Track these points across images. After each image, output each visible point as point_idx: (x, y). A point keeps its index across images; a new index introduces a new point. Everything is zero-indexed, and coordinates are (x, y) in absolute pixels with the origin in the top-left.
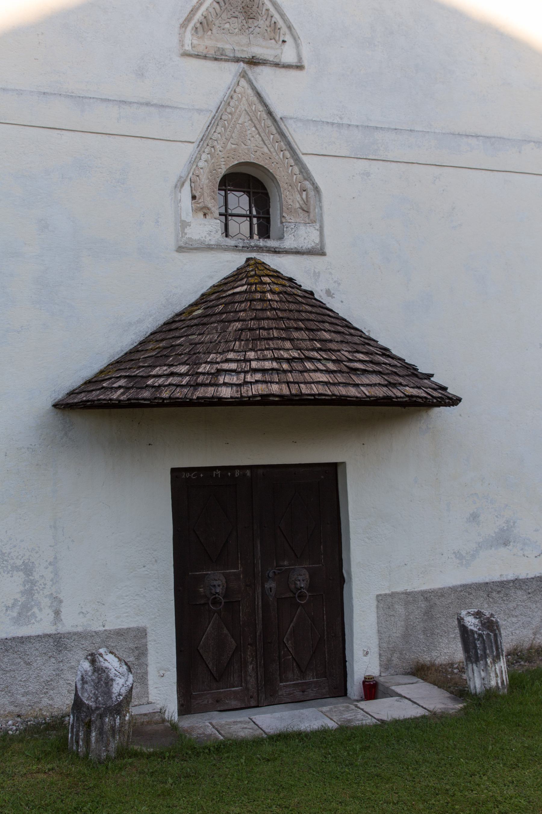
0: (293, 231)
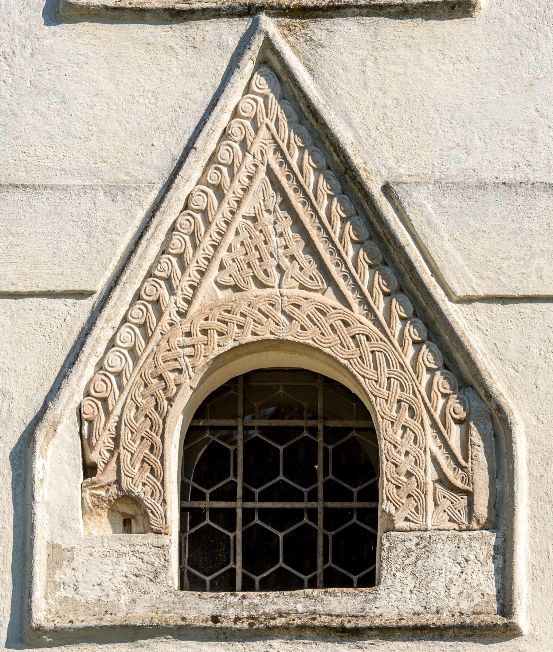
0: (413, 558)
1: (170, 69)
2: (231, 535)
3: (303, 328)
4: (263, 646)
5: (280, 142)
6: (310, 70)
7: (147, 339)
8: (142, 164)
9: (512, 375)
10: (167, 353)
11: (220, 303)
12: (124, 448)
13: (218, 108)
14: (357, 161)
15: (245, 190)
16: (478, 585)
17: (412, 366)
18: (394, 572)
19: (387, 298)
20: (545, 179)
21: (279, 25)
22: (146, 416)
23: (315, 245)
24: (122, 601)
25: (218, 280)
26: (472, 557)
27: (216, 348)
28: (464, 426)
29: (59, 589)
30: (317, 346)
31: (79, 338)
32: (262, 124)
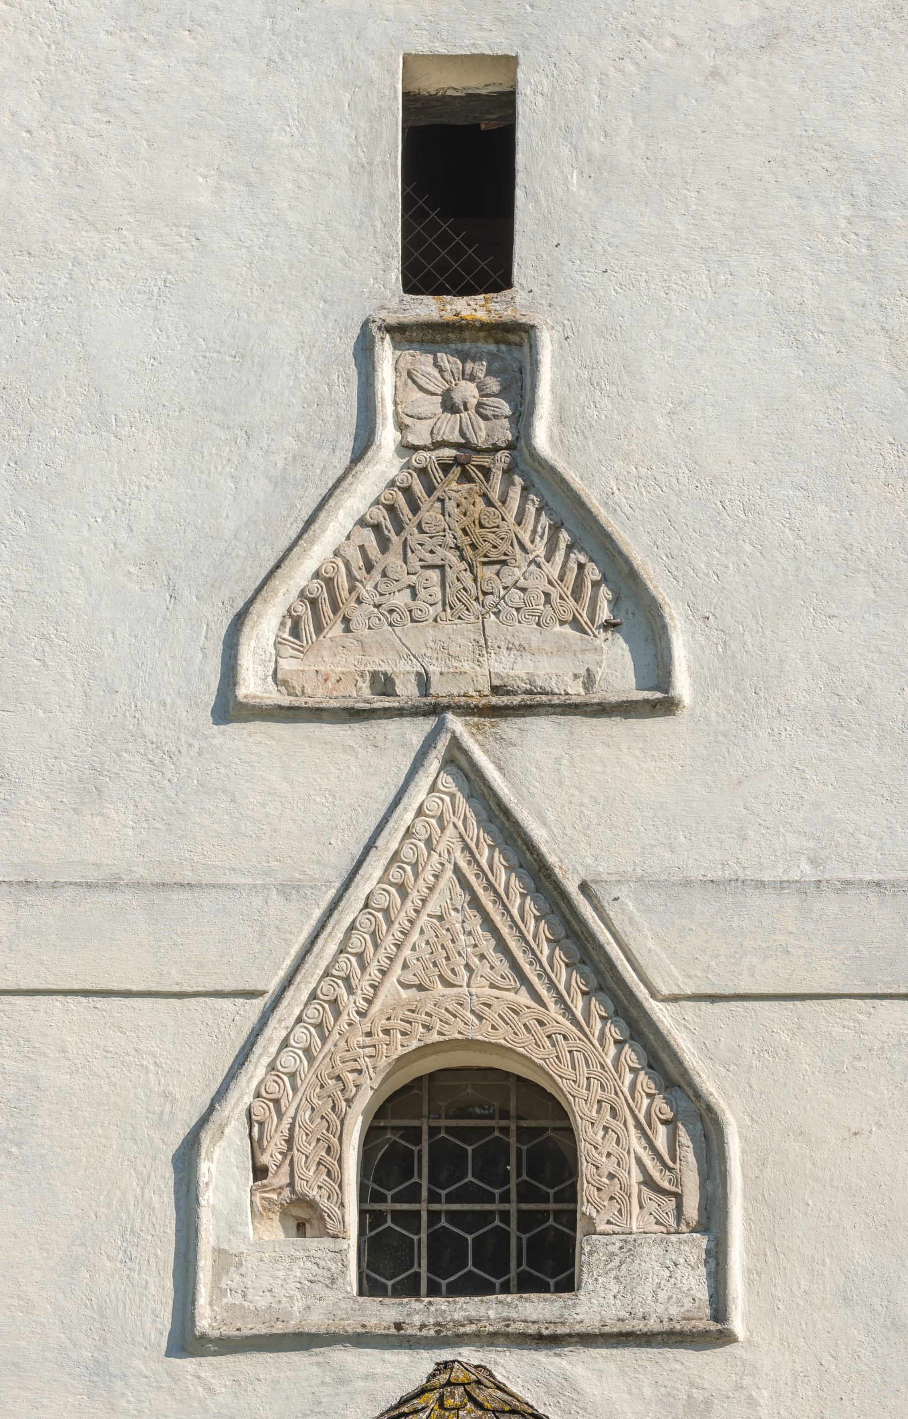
0: (616, 1262)
1: (349, 768)
2: (415, 1238)
3: (493, 1027)
4: (451, 1354)
5: (468, 841)
6: (500, 769)
7: (324, 1039)
8: (318, 863)
9: (723, 1074)
10: (346, 1053)
11: (403, 1003)
12: (298, 1150)
13: (401, 807)
14: (552, 859)
15: (431, 889)
16: (689, 1290)
17: (614, 1066)
18: (595, 1276)
19: (586, 997)
20: (756, 877)
21: (467, 724)
22: (323, 1117)
23: (507, 944)
24: (295, 1308)
25: (401, 979)
26: (682, 1261)
27: (399, 1048)
28: (671, 1126)
29: (225, 1296)
30: (509, 1045)
31: (249, 1038)
32: (448, 822)
